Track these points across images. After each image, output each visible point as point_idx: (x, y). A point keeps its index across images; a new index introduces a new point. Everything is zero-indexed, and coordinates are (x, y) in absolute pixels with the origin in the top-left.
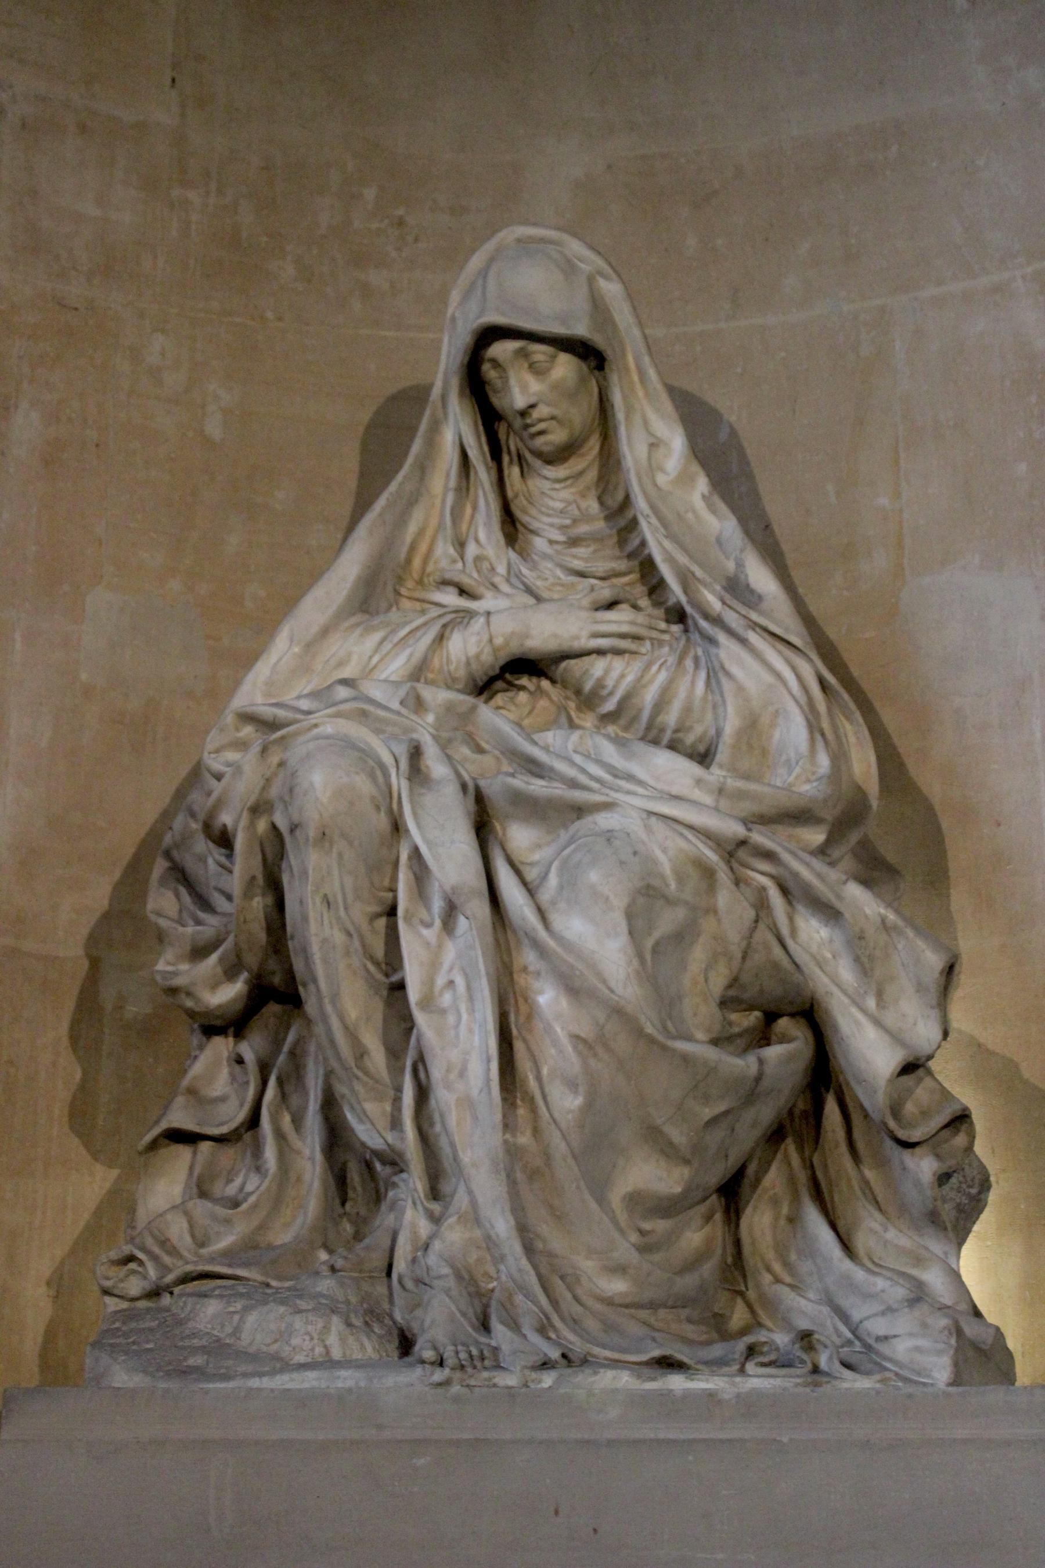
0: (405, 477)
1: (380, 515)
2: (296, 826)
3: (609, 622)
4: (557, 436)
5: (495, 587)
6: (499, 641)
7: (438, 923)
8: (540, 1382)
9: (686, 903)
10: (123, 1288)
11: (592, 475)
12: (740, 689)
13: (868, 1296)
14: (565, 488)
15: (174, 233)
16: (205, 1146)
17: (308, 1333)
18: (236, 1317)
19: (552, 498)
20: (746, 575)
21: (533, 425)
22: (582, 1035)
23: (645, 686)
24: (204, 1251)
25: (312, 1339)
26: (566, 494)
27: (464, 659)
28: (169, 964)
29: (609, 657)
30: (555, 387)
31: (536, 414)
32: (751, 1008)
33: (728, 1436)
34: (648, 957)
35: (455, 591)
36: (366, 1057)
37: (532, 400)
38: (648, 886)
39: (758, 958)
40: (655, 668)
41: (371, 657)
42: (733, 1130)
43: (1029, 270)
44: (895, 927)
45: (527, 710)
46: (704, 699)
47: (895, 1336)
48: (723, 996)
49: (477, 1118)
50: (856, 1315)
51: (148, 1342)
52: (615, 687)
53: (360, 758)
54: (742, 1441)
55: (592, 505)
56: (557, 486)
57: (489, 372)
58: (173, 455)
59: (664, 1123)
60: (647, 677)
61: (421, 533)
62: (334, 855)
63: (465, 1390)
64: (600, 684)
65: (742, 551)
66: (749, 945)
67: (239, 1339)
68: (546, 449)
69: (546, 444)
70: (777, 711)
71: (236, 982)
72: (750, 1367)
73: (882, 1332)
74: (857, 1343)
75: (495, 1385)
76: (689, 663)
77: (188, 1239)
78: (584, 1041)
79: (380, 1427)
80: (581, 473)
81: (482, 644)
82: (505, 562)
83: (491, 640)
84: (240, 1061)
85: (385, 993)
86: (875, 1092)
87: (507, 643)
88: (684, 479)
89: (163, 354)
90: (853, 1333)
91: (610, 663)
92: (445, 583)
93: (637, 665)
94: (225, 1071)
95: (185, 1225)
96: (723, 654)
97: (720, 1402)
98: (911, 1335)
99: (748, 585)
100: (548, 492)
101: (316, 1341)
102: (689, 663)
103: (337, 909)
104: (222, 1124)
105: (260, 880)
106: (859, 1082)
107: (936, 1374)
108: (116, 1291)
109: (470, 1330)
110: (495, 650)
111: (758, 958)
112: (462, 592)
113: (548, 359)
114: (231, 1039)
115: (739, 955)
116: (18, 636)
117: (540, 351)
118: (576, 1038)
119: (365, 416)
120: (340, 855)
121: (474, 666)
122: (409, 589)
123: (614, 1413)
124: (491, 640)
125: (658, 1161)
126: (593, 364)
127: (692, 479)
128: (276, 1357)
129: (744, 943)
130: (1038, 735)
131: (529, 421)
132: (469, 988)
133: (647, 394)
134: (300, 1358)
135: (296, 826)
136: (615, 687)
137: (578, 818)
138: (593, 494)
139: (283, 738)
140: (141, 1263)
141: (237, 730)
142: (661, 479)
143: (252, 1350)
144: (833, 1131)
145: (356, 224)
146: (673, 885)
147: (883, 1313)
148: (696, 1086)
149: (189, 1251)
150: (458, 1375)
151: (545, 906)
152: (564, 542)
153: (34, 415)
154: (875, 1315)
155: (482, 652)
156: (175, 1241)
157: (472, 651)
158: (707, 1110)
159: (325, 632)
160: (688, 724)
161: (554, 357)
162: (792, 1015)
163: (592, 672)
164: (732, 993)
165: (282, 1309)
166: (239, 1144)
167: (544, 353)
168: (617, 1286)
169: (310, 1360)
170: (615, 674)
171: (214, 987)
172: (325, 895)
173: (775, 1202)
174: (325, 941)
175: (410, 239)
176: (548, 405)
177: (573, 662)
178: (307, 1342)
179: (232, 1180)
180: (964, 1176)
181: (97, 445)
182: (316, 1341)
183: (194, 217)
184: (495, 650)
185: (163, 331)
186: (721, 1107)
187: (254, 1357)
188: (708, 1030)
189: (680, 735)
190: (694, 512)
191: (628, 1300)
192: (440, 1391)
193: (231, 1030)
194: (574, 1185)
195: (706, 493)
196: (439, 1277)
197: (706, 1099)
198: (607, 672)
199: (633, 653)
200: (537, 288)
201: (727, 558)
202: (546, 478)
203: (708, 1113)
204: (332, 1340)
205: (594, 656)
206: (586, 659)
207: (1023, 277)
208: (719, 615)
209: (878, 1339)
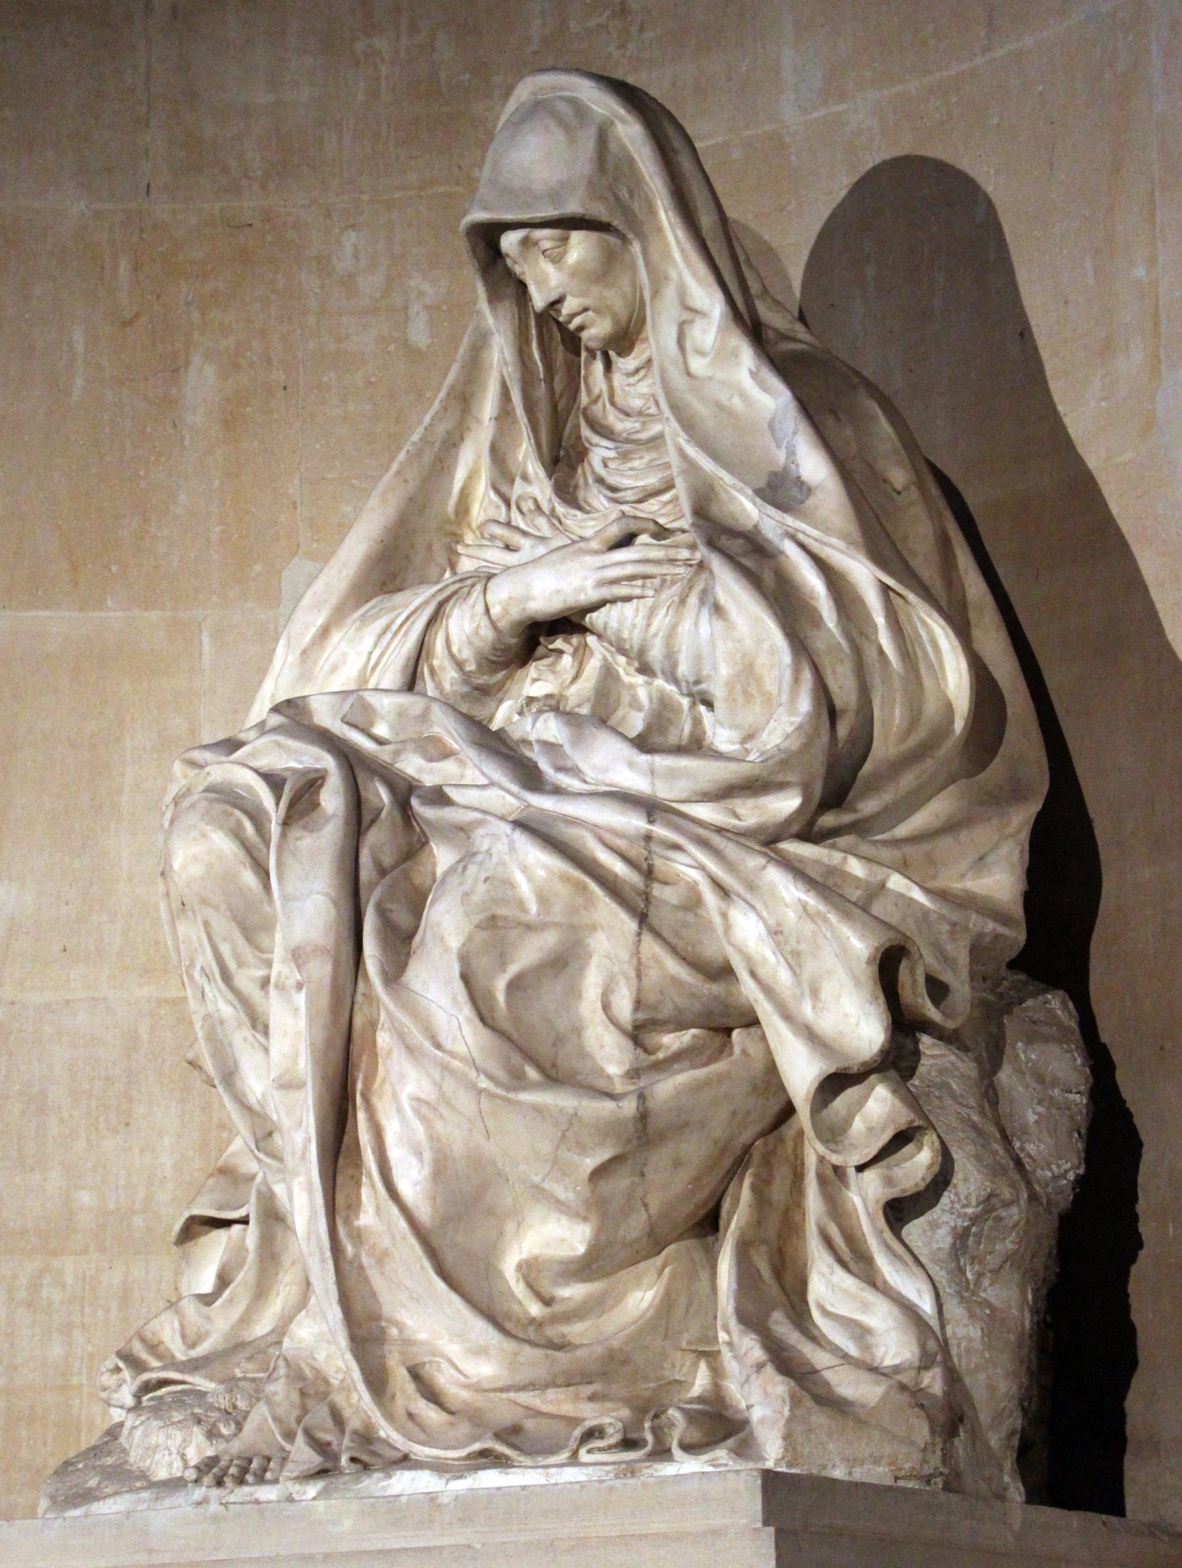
0: (433, 419)
1: (398, 473)
8: (304, 1493)
9: (556, 925)
14: (639, 381)
15: (361, 97)
22: (423, 1096)
25: (170, 1454)
30: (574, 273)
31: (566, 309)
32: (682, 1026)
33: (422, 1545)
34: (501, 997)
36: (277, 1137)
37: (554, 297)
38: (493, 917)
41: (371, 653)
42: (642, 1175)
44: (819, 913)
45: (569, 677)
48: (635, 1021)
53: (224, 812)
54: (441, 1548)
58: (373, 380)
59: (543, 1180)
61: (471, 477)
65: (795, 433)
75: (257, 1502)
76: (693, 600)
77: (179, 1340)
78: (428, 1103)
79: (150, 1551)
87: (506, 611)
89: (356, 257)
99: (799, 478)
101: (174, 1455)
102: (693, 600)
109: (279, 1438)
111: (652, 975)
113: (558, 243)
115: (633, 974)
116: (205, 638)
120: (206, 924)
121: (478, 643)
122: (468, 545)
124: (487, 610)
125: (558, 1220)
127: (735, 354)
129: (635, 961)
142: (697, 365)
145: (574, 26)
146: (533, 908)
148: (564, 1136)
150: (215, 1492)
153: (210, 370)
155: (478, 627)
158: (588, 1160)
159: (324, 633)
161: (565, 240)
164: (641, 1016)
167: (548, 239)
168: (485, 1370)
174: (207, 1017)
177: (595, 615)
180: (956, 1194)
181: (285, 388)
182: (174, 1455)
183: (384, 70)
185: (353, 226)
186: (605, 1155)
188: (621, 1062)
189: (703, 686)
190: (743, 395)
191: (499, 1384)
192: (201, 1510)
197: (582, 1149)
201: (779, 446)
203: (590, 1163)
208: (755, 526)
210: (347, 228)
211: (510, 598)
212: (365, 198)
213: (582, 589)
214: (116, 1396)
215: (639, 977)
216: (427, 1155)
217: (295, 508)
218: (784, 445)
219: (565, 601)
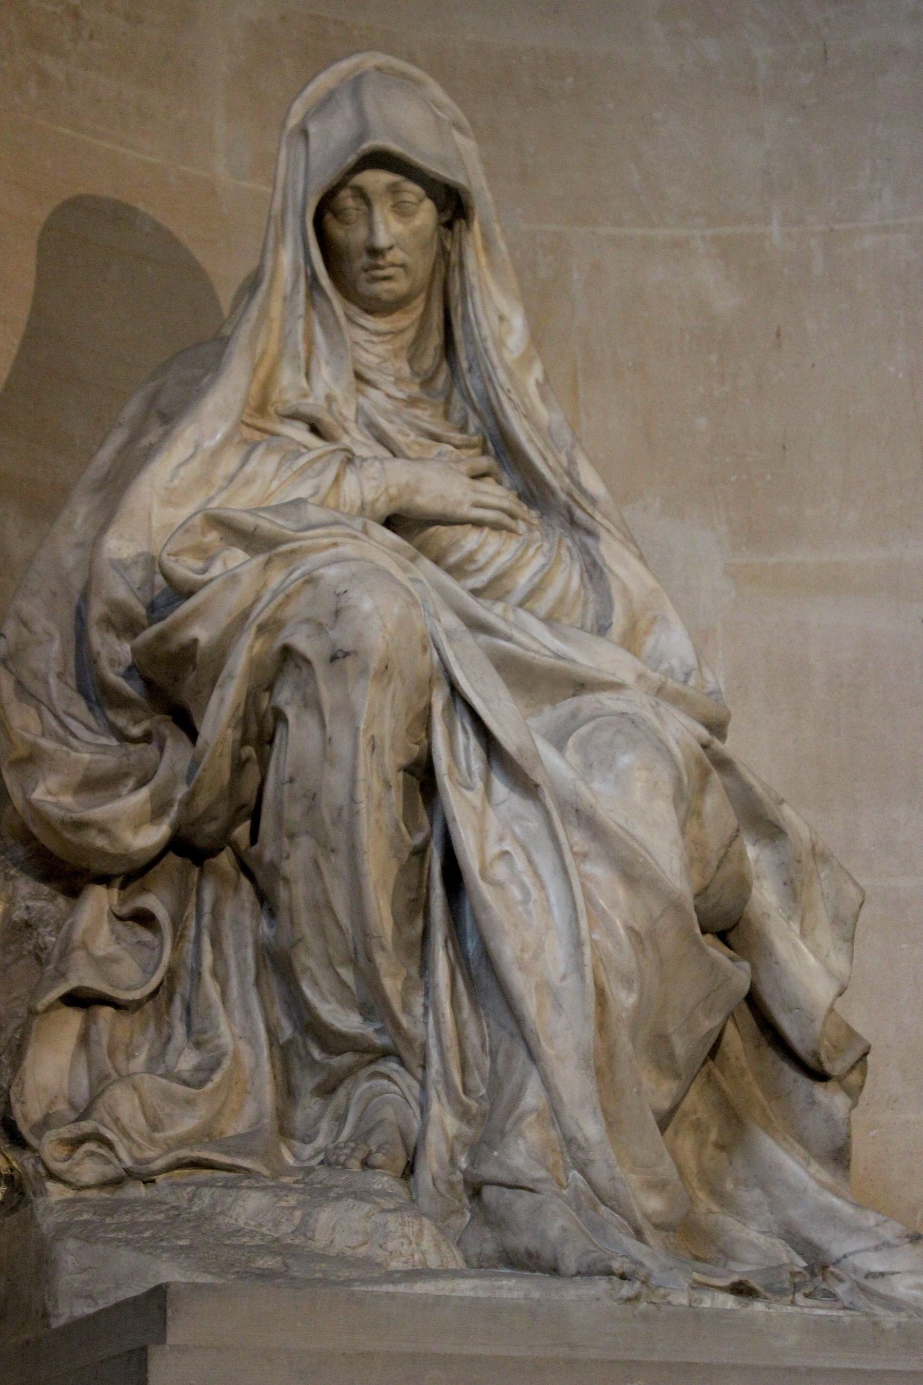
2: (347, 654)
3: (486, 493)
4: (400, 286)
5: (346, 431)
6: (393, 491)
7: (479, 785)
10: (77, 1173)
11: (410, 335)
12: (625, 590)
13: (857, 1230)
14: (382, 342)
16: (106, 1012)
17: (404, 1236)
18: (298, 1214)
19: (366, 351)
20: (578, 473)
21: (378, 267)
22: (637, 927)
23: (520, 568)
24: (158, 1136)
25: (410, 1243)
26: (380, 349)
27: (358, 503)
28: (49, 792)
29: (486, 530)
39: (730, 869)
40: (531, 551)
43: (709, 232)
46: (578, 594)
47: (893, 1273)
49: (560, 1006)
51: (179, 1238)
52: (488, 563)
55: (406, 370)
56: (375, 339)
57: (347, 200)
60: (526, 558)
62: (390, 694)
63: (652, 1307)
64: (470, 558)
65: (573, 447)
66: (726, 854)
67: (312, 1239)
68: (386, 297)
69: (389, 291)
70: (655, 617)
71: (160, 824)
72: (799, 1298)
73: (877, 1267)
77: (142, 1120)
80: (402, 331)
81: (379, 492)
82: (353, 408)
83: (387, 489)
84: (145, 919)
85: (406, 855)
86: (812, 1021)
88: (525, 361)
91: (486, 538)
92: (295, 416)
93: (513, 546)
94: (106, 927)
95: (137, 1102)
96: (603, 548)
97: (883, 1331)
98: (912, 1272)
100: (362, 343)
102: (564, 551)
103: (382, 755)
104: (128, 989)
105: (240, 713)
108: (68, 1177)
110: (391, 500)
112: (315, 429)
114: (115, 891)
115: (715, 863)
117: (412, 191)
118: (630, 930)
119: (42, 215)
123: (792, 1339)
126: (445, 219)
128: (368, 1262)
129: (722, 853)
131: (381, 262)
132: (530, 861)
133: (492, 264)
134: (396, 1265)
135: (347, 654)
136: (488, 563)
137: (574, 695)
138: (404, 354)
139: (293, 552)
140: (109, 1145)
141: (203, 534)
143: (333, 1252)
144: (737, 1058)
147: (877, 1249)
149: (141, 1135)
152: (403, 400)
154: (867, 1250)
155: (377, 499)
156: (125, 1120)
157: (370, 497)
160: (557, 615)
161: (421, 201)
162: (712, 933)
163: (463, 543)
165: (367, 1207)
166: (137, 1014)
169: (410, 1267)
170: (490, 550)
171: (136, 828)
172: (373, 737)
173: (698, 1127)
175: (85, 34)
176: (402, 249)
177: (442, 529)
178: (405, 1247)
179: (134, 1056)
184: (391, 500)
187: (342, 1260)
192: (629, 1307)
193: (118, 882)
194: (635, 1090)
195: (541, 379)
196: (539, 1180)
198: (481, 546)
199: (511, 531)
200: (417, 123)
202: (363, 328)
204: (427, 1243)
205: (469, 526)
206: (458, 528)
207: (703, 238)
209: (870, 1275)
211: (407, 485)
213: (460, 503)
214: (77, 1169)
215: (718, 867)
216: (636, 986)
218: (564, 451)
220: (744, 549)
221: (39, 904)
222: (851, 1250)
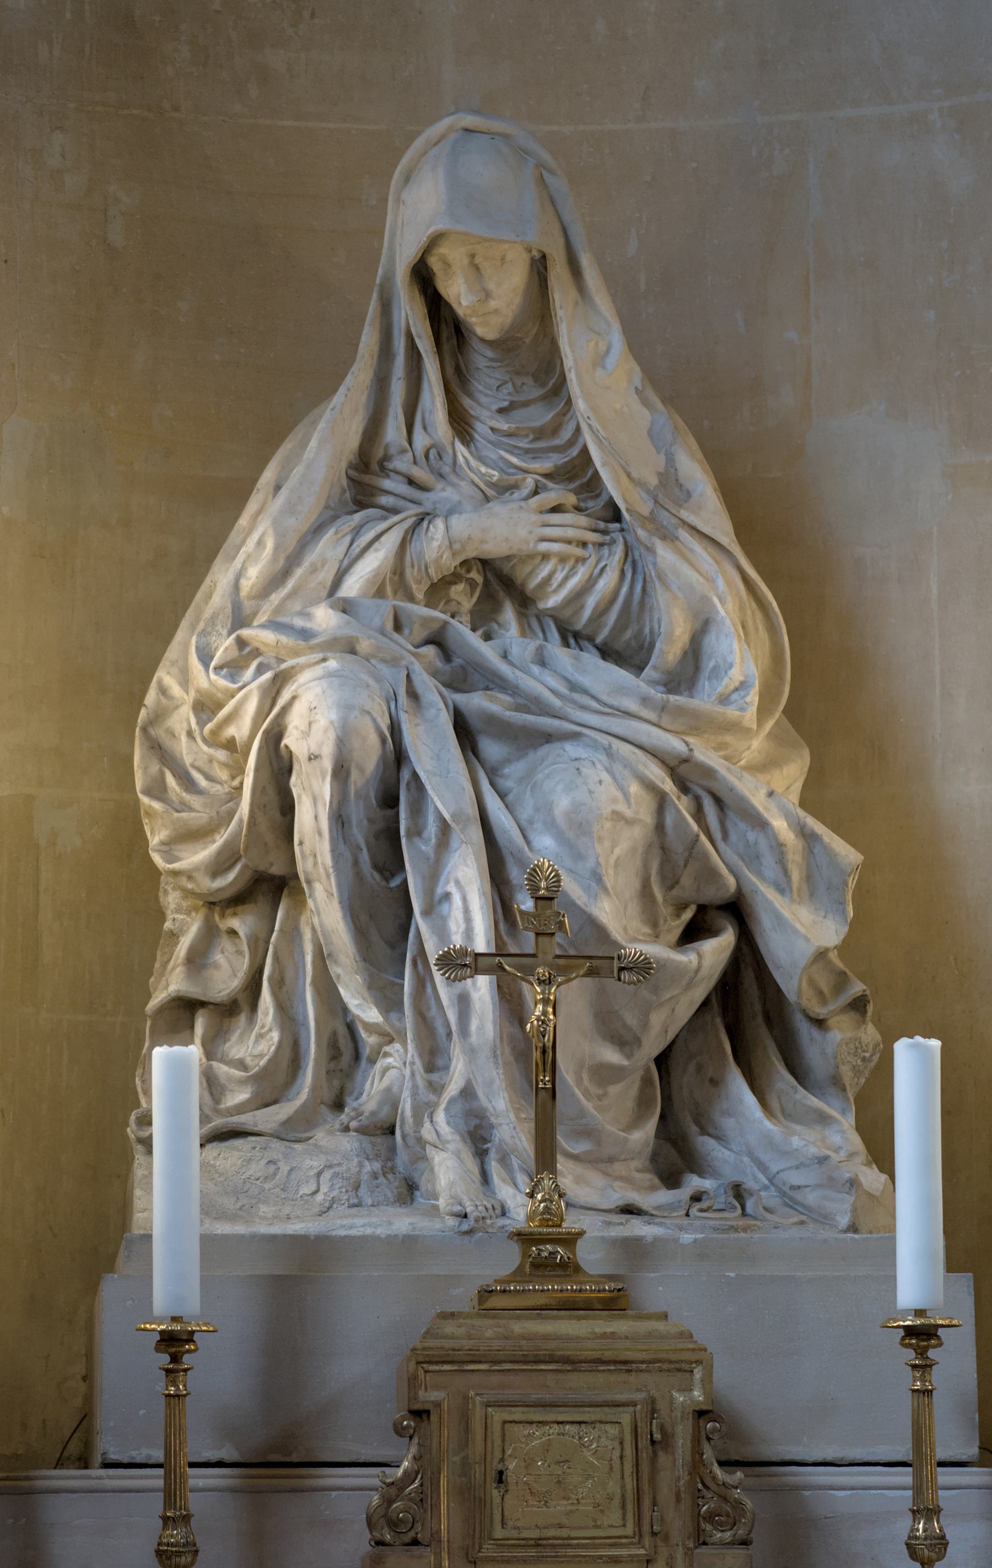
15: (68, 15)
35: (406, 480)
47: (806, 1186)
50: (774, 1168)
58: (77, 268)
73: (796, 1182)
74: (773, 1189)
86: (791, 978)
90: (771, 1181)
106: (778, 968)
107: (838, 1218)
129: (686, 853)
130: (935, 592)
147: (797, 1167)
151: (524, 824)
154: (791, 1168)
175: (306, 14)
195: (640, 387)
209: (793, 1188)
210: (57, 128)
212: (72, 105)
217: (13, 369)
219: (511, 548)
220: (963, 448)
221: (181, 917)
222: (782, 1168)
